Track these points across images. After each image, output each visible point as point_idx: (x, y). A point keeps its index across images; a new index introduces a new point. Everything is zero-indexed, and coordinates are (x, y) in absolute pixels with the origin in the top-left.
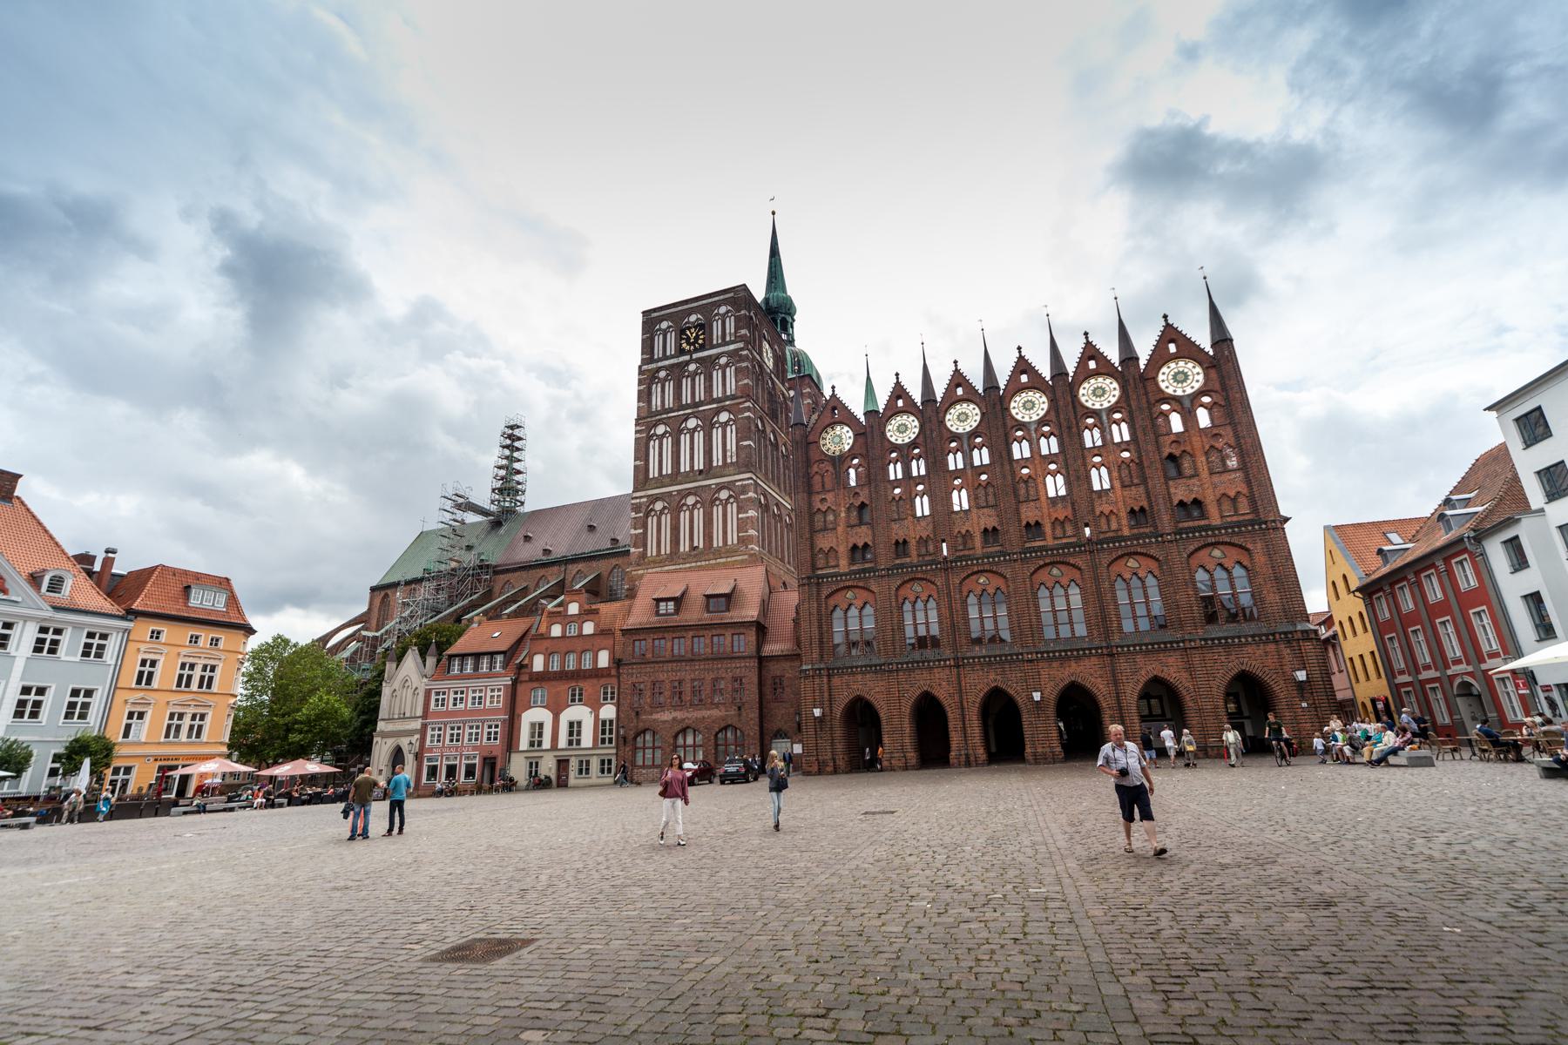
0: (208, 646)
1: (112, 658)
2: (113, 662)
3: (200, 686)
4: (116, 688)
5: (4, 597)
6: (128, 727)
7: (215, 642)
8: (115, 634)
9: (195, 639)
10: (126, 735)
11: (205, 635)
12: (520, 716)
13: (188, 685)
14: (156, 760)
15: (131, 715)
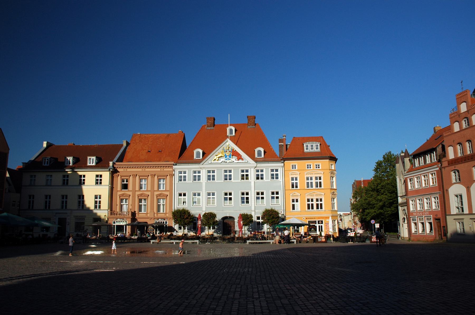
0: (315, 168)
1: (281, 179)
2: (282, 180)
3: (317, 186)
4: (285, 190)
5: (243, 161)
6: (293, 206)
7: (318, 166)
8: (279, 169)
9: (309, 166)
10: (293, 208)
11: (313, 163)
12: (447, 190)
13: (312, 186)
14: (307, 218)
15: (293, 201)
